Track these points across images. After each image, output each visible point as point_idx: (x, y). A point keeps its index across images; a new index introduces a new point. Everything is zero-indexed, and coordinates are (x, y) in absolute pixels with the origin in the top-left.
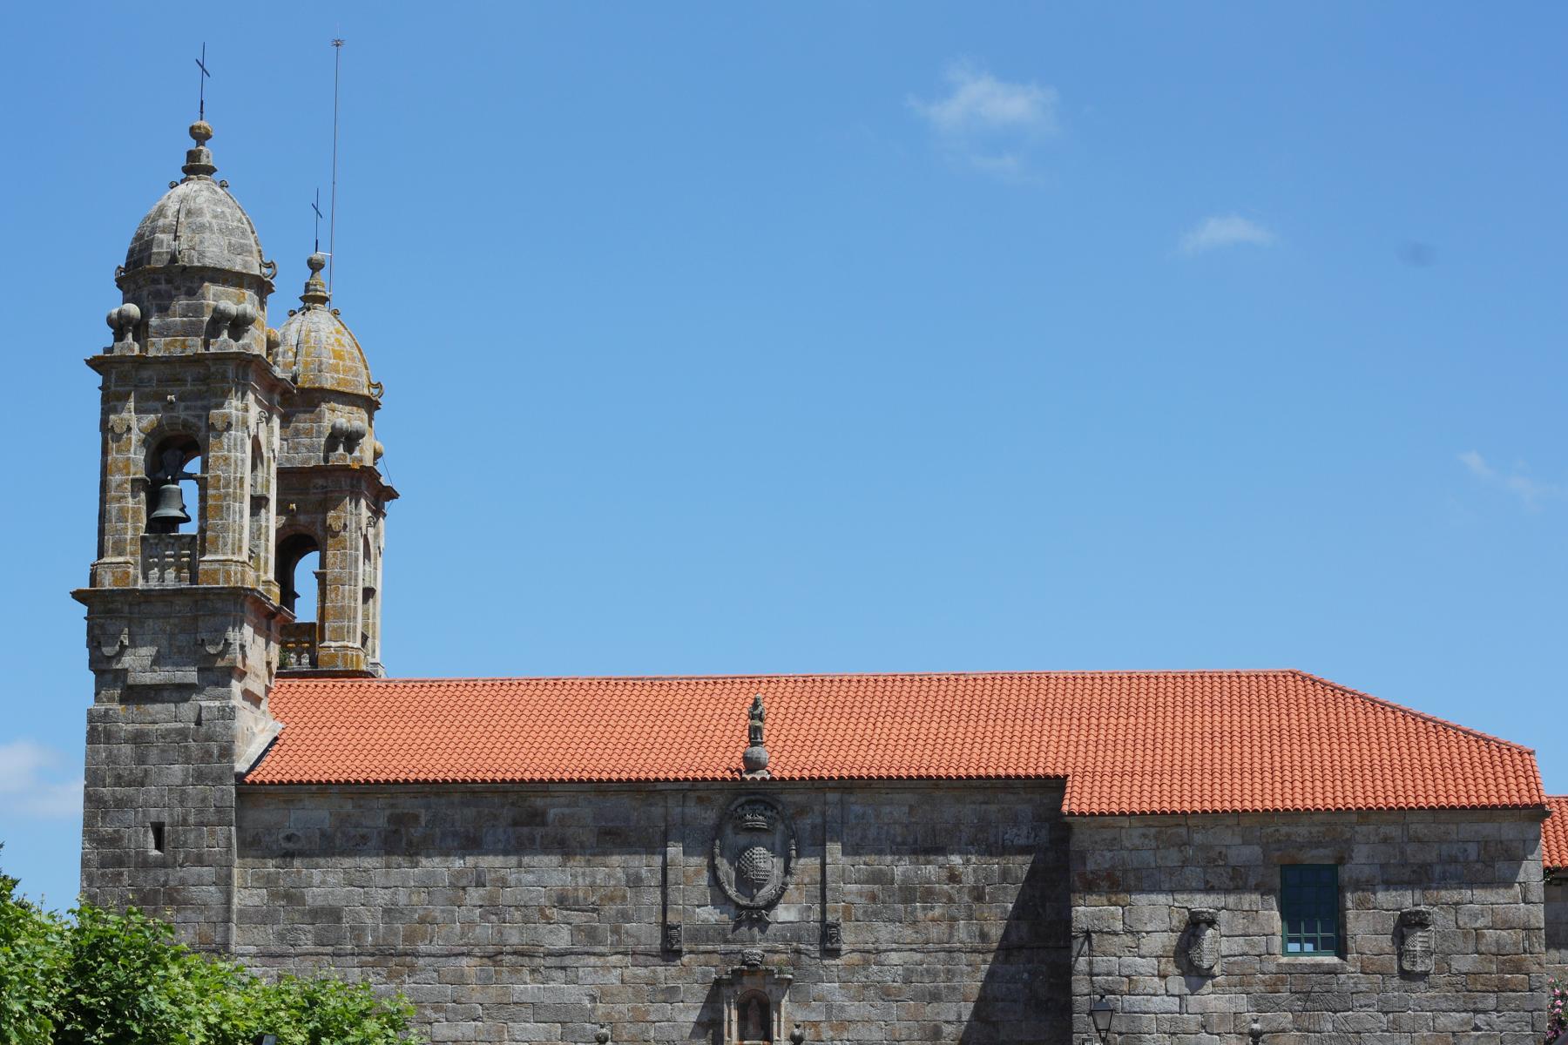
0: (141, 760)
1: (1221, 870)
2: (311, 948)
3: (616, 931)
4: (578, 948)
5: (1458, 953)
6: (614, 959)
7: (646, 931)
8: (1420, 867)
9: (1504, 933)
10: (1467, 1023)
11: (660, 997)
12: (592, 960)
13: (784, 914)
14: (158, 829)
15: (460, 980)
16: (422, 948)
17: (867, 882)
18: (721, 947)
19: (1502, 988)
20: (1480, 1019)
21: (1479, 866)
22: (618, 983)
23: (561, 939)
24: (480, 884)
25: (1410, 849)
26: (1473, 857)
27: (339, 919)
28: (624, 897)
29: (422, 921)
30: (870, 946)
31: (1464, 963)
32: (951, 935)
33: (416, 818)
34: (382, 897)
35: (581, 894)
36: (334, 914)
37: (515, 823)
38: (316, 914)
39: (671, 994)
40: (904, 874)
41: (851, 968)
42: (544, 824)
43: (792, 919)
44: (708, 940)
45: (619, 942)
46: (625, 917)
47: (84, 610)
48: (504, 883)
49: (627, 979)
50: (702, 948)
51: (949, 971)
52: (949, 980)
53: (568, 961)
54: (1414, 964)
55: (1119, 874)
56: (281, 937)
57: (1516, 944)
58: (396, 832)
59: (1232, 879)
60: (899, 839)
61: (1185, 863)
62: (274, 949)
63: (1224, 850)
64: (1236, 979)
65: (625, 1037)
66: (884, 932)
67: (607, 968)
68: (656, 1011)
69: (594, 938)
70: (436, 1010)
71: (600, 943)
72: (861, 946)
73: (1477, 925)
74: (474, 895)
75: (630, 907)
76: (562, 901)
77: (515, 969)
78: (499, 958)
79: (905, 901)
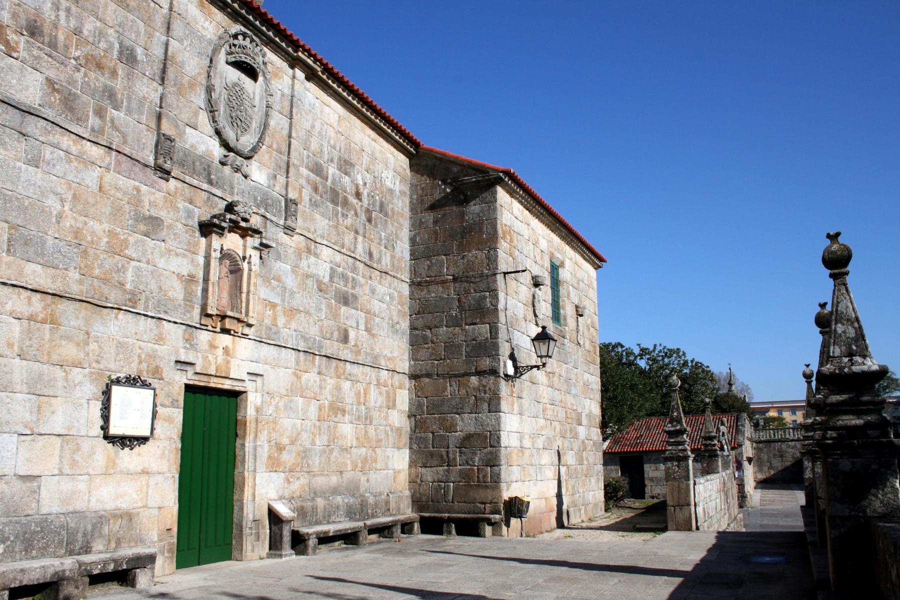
6: (95, 152)
11: (142, 227)
12: (66, 141)
22: (96, 188)
28: (114, 73)
35: (61, 37)
43: (262, 182)
44: (194, 173)
45: (101, 131)
49: (106, 187)
53: (34, 126)
65: (97, 272)
69: (71, 109)
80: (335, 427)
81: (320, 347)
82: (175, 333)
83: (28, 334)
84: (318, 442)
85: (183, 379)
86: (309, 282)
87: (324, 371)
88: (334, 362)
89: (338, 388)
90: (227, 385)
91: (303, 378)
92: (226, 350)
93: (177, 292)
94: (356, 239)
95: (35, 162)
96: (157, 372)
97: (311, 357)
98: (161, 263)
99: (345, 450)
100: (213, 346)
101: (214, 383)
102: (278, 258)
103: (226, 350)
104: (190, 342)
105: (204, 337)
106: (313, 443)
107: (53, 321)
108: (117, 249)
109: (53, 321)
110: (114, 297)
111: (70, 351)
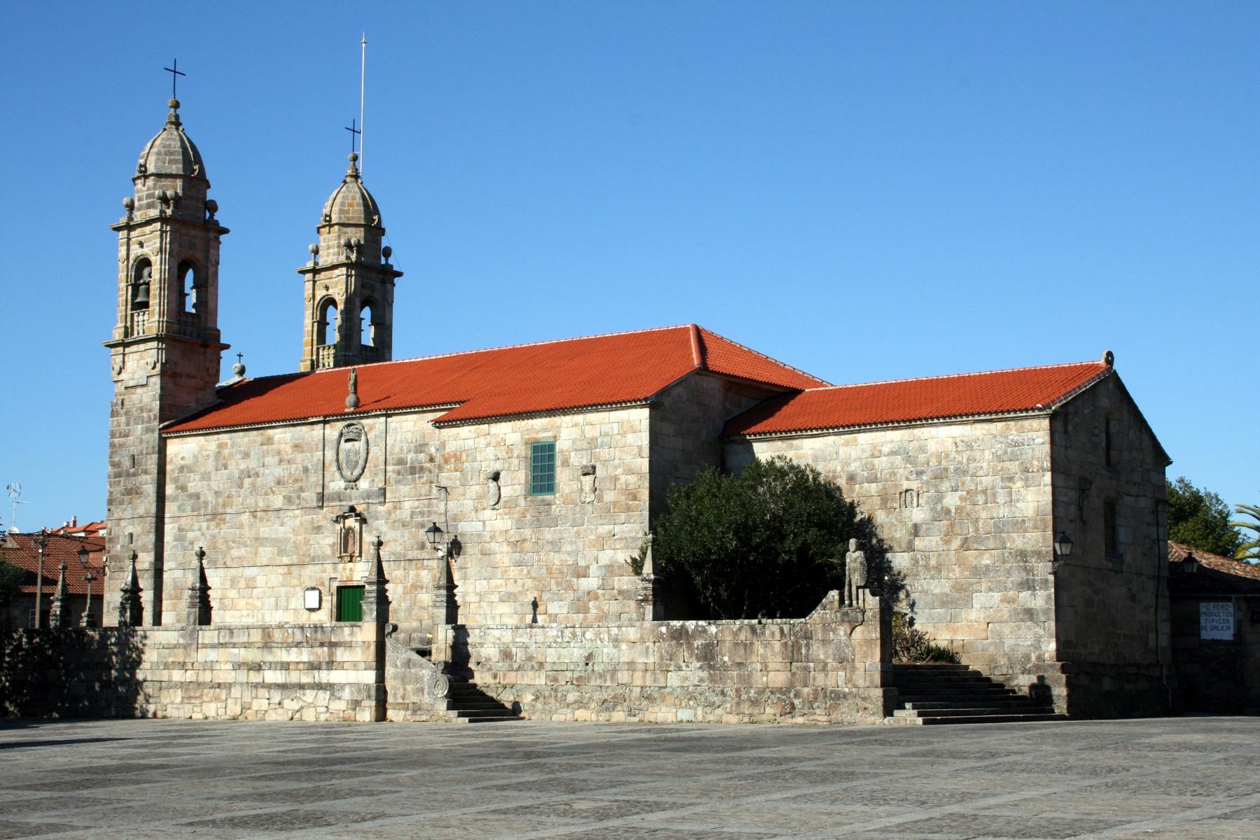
0: (128, 425)
1: (502, 448)
2: (189, 513)
3: (299, 497)
4: (285, 507)
5: (608, 489)
6: (297, 512)
7: (310, 496)
8: (592, 439)
9: (629, 477)
10: (610, 532)
12: (290, 513)
13: (363, 484)
14: (133, 457)
15: (241, 526)
16: (228, 511)
17: (396, 465)
18: (338, 503)
19: (628, 509)
20: (617, 529)
21: (619, 437)
23: (278, 501)
24: (249, 477)
25: (587, 428)
26: (616, 432)
27: (198, 498)
28: (302, 480)
29: (228, 497)
30: (397, 500)
31: (609, 496)
32: (430, 491)
33: (226, 444)
34: (214, 486)
36: (197, 496)
37: (262, 444)
38: (191, 496)
39: (318, 529)
40: (411, 459)
41: (389, 513)
42: (272, 444)
44: (333, 500)
46: (302, 489)
47: (223, 340)
48: (257, 475)
50: (331, 504)
51: (429, 511)
52: (429, 516)
53: (281, 514)
54: (586, 497)
55: (458, 453)
56: (179, 508)
57: (635, 483)
58: (219, 452)
59: (507, 453)
60: (410, 440)
61: (488, 445)
62: (177, 514)
63: (504, 436)
64: (507, 510)
66: (405, 489)
67: (295, 517)
68: (313, 538)
70: (233, 542)
71: (293, 504)
72: (394, 500)
73: (617, 473)
74: (247, 481)
75: (303, 484)
76: (279, 483)
77: (261, 520)
78: (223, 516)
79: (412, 474)
80: (415, 597)
81: (405, 555)
82: (329, 567)
83: (284, 579)
84: (403, 605)
85: (335, 584)
86: (397, 524)
87: (407, 567)
88: (414, 562)
89: (418, 575)
90: (355, 584)
91: (393, 575)
92: (351, 569)
93: (328, 551)
94: (431, 487)
95: (282, 525)
96: (323, 584)
97: (398, 563)
98: (322, 542)
99: (422, 608)
100: (344, 569)
101: (349, 584)
102: (377, 519)
103: (351, 569)
104: (335, 570)
105: (341, 566)
106: (400, 605)
107: (289, 573)
108: (307, 542)
109: (289, 573)
110: (307, 560)
111: (295, 582)
